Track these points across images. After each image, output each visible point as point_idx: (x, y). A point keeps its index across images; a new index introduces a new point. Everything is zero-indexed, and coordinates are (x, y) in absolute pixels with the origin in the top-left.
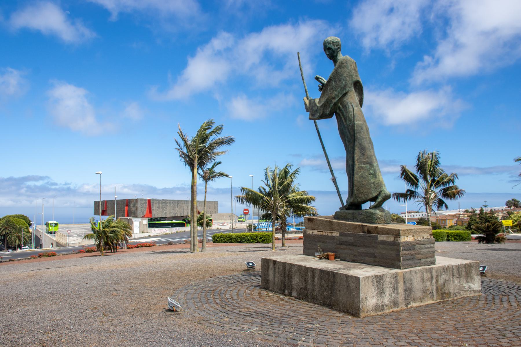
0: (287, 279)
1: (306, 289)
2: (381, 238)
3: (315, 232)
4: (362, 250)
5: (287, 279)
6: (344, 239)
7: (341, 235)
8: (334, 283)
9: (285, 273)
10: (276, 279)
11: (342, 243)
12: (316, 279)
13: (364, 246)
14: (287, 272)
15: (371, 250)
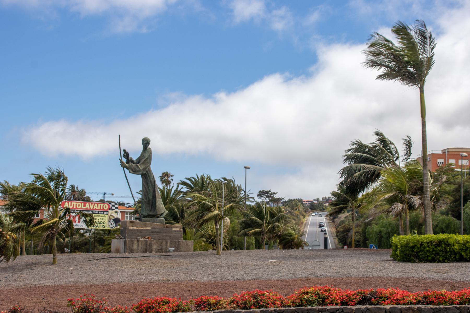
0: (148, 247)
1: (161, 249)
2: (174, 229)
3: (135, 228)
4: (164, 234)
5: (148, 247)
6: (154, 230)
7: (152, 228)
8: (179, 244)
9: (146, 244)
10: (140, 248)
11: (152, 232)
12: (168, 245)
13: (166, 233)
14: (148, 244)
15: (169, 234)
